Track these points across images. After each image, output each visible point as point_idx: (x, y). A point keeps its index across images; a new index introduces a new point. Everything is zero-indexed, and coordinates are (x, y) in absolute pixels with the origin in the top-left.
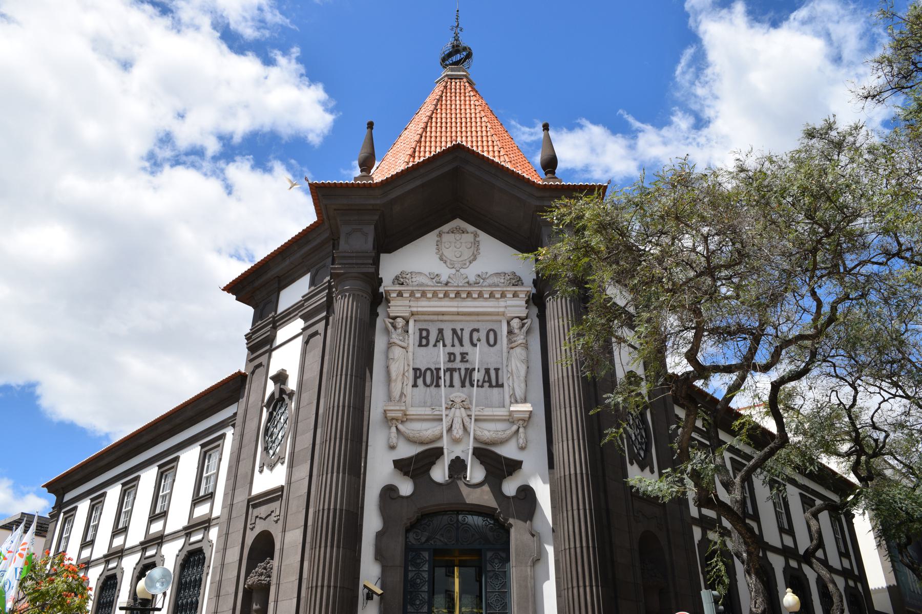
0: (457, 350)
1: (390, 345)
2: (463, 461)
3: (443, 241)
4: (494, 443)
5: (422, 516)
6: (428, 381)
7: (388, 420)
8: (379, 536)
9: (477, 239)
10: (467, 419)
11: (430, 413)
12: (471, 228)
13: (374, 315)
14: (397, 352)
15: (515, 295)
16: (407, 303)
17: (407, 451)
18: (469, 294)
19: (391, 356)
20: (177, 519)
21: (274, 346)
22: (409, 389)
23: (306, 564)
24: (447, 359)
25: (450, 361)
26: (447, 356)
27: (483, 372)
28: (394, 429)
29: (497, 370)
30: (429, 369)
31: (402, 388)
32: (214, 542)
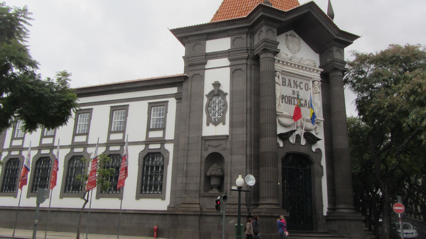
2: (300, 136)
3: (288, 39)
4: (311, 130)
5: (287, 154)
6: (287, 101)
9: (300, 42)
11: (289, 114)
12: (297, 36)
16: (280, 66)
21: (207, 67)
22: (281, 103)
24: (292, 93)
26: (292, 92)
27: (304, 101)
30: (287, 96)
31: (279, 103)
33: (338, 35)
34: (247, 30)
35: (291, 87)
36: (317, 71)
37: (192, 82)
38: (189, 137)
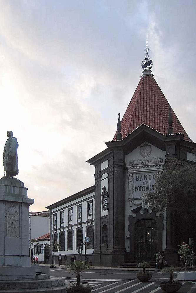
0: (146, 181)
7: (130, 200)
8: (129, 226)
13: (125, 173)
14: (130, 183)
16: (132, 170)
17: (134, 207)
20: (84, 219)
28: (131, 202)
30: (139, 187)
34: (113, 155)
36: (160, 165)
38: (97, 218)
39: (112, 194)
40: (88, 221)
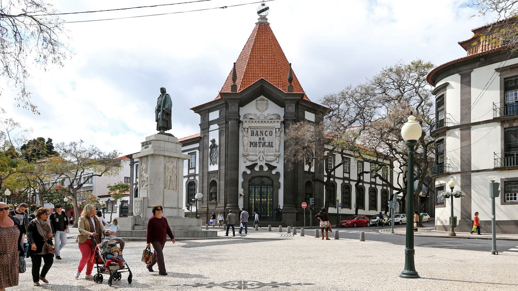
1: (244, 136)
6: (254, 146)
7: (244, 156)
8: (242, 183)
10: (264, 156)
12: (266, 99)
13: (239, 127)
14: (245, 138)
15: (278, 122)
16: (248, 124)
17: (249, 164)
18: (265, 122)
19: (244, 139)
22: (249, 148)
23: (226, 189)
25: (259, 140)
28: (245, 158)
29: (272, 142)
32: (198, 180)
33: (285, 96)
35: (258, 135)
37: (203, 140)
39: (223, 148)
40: (189, 176)
